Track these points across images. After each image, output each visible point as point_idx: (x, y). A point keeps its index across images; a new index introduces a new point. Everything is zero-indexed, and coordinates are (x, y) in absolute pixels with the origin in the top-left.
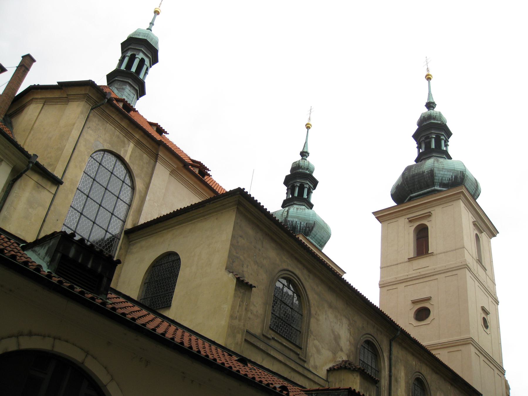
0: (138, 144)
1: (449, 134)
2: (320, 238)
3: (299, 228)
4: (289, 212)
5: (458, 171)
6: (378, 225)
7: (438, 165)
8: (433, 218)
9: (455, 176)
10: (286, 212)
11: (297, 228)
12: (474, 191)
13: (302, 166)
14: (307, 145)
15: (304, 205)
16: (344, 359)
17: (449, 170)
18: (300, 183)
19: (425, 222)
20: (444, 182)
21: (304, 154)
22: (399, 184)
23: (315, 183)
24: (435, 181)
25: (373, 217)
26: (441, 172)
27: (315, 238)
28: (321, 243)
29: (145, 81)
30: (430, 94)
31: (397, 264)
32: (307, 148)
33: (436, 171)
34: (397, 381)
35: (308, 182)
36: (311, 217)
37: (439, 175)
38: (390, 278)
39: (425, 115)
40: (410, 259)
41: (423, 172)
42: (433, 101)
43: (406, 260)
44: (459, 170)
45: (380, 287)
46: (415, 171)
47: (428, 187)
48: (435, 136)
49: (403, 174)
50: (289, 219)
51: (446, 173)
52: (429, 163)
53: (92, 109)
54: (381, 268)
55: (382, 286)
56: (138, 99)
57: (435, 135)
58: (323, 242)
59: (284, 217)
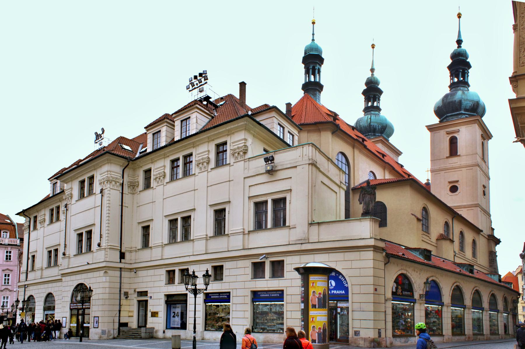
3: (377, 129)
4: (372, 119)
5: (475, 101)
6: (428, 133)
8: (460, 133)
15: (377, 111)
17: (470, 101)
19: (455, 135)
22: (440, 106)
24: (462, 107)
25: (426, 128)
26: (466, 102)
33: (463, 101)
35: (378, 94)
36: (384, 122)
37: (465, 104)
38: (437, 167)
40: (447, 157)
41: (455, 101)
44: (476, 100)
45: (431, 172)
46: (450, 99)
47: (457, 110)
50: (372, 124)
51: (468, 102)
52: (459, 94)
54: (431, 161)
59: (368, 123)
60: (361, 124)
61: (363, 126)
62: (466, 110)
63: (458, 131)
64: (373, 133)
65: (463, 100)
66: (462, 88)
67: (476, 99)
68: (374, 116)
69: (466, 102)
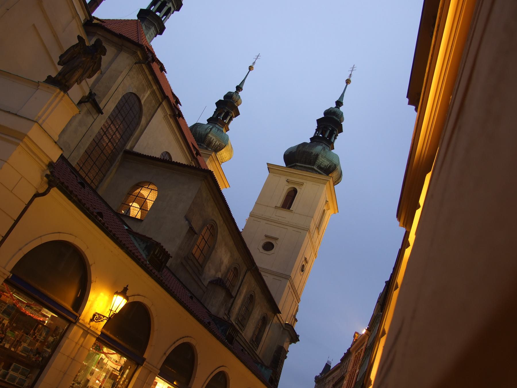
0: (153, 93)
1: (341, 131)
2: (224, 157)
3: (213, 144)
4: (212, 130)
7: (323, 153)
9: (329, 166)
10: (210, 129)
11: (212, 144)
12: (336, 180)
13: (233, 98)
14: (244, 83)
16: (219, 277)
17: (328, 160)
18: (227, 110)
20: (322, 166)
21: (239, 88)
22: (293, 152)
23: (237, 114)
24: (316, 162)
27: (221, 155)
28: (223, 160)
29: (166, 24)
30: (342, 95)
31: (268, 206)
32: (243, 85)
33: (320, 157)
34: (240, 295)
37: (321, 160)
39: (332, 110)
41: (312, 153)
42: (341, 101)
43: (274, 206)
44: (334, 162)
48: (331, 129)
49: (299, 146)
51: (325, 161)
52: (318, 149)
53: (136, 63)
55: (252, 215)
56: (156, 36)
57: (332, 129)
58: (224, 160)
59: (207, 132)
60: (198, 129)
61: (199, 133)
62: (320, 167)
63: (302, 184)
64: (207, 146)
65: (320, 155)
66: (324, 145)
67: (335, 161)
68: (217, 129)
69: (323, 159)
